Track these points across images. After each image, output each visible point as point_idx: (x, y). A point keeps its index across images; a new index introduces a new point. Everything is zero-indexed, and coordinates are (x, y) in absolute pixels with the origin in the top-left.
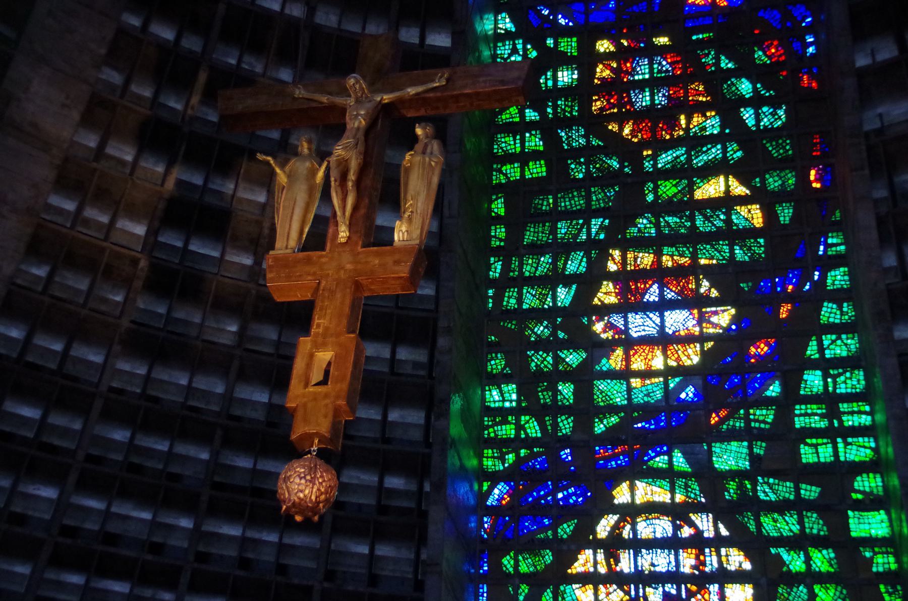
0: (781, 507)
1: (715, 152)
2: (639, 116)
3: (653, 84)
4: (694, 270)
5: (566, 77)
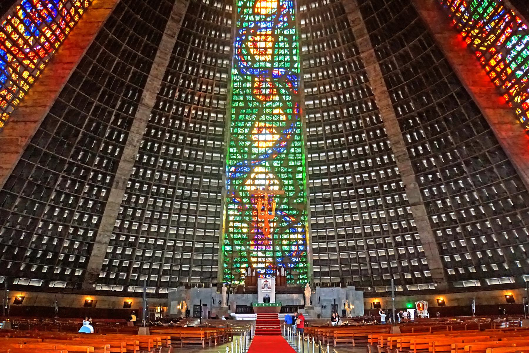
0: (285, 173)
1: (277, 104)
2: (263, 95)
3: (266, 88)
4: (272, 127)
5: (249, 85)
